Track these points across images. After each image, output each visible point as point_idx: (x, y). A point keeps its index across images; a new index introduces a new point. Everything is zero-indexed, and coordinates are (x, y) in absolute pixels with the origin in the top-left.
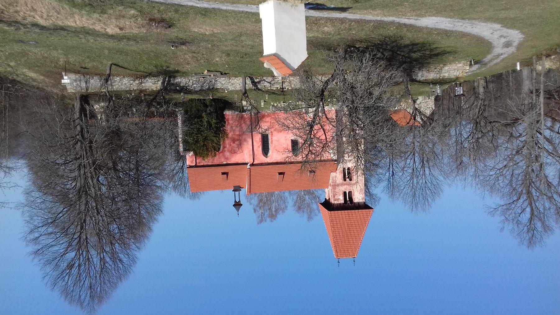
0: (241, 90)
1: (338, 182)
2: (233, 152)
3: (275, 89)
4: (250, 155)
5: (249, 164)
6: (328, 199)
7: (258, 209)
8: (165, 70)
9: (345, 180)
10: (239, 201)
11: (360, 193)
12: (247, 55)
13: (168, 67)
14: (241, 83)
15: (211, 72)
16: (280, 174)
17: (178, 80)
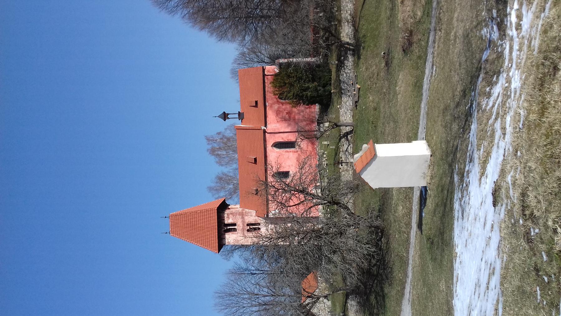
0: (339, 121)
1: (246, 218)
2: (278, 112)
3: (341, 155)
4: (275, 129)
5: (265, 128)
6: (229, 207)
7: (221, 136)
8: (361, 46)
9: (248, 225)
10: (228, 118)
11: (235, 240)
12: (375, 128)
13: (363, 48)
14: (347, 121)
15: (358, 91)
16: (255, 159)
17: (351, 58)
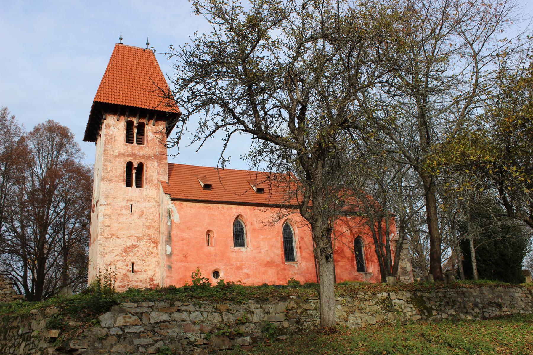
1: (156, 163)
9: (141, 166)
11: (112, 137)
